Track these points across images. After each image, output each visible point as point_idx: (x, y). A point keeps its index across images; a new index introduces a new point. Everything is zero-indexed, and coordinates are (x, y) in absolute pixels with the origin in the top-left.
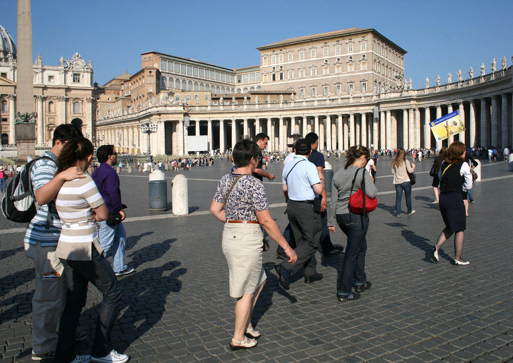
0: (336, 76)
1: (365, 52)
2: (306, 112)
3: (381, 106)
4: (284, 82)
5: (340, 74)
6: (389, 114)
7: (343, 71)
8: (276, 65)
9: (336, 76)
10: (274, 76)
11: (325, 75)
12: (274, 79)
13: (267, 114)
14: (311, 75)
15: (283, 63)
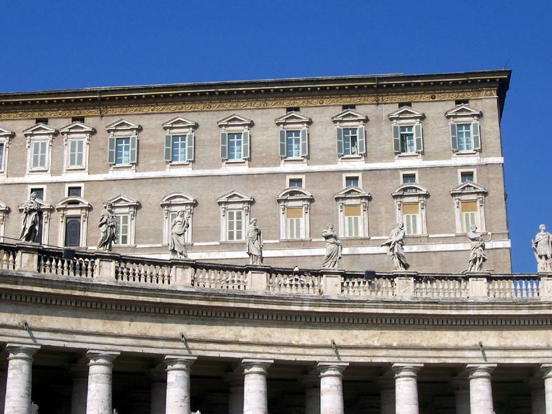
1: (473, 160)
2: (491, 338)
5: (365, 241)
7: (373, 228)
8: (47, 177)
11: (291, 243)
13: (247, 333)
14: (224, 237)
15: (84, 176)
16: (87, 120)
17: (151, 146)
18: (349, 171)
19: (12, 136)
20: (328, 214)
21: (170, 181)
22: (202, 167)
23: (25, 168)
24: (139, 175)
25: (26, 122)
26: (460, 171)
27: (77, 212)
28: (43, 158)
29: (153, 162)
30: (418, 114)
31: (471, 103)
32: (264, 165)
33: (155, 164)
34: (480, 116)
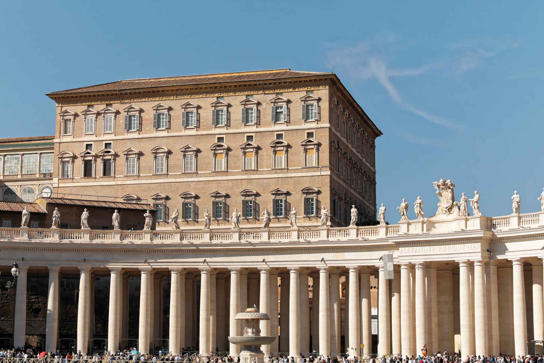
0: (245, 177)
3: (403, 251)
4: (113, 183)
6: (419, 273)
8: (93, 138)
9: (245, 177)
10: (88, 166)
12: (87, 173)
15: (112, 137)
16: (114, 105)
17: (147, 119)
18: (248, 133)
19: (76, 115)
20: (236, 157)
21: (157, 139)
22: (173, 132)
23: (83, 133)
24: (140, 136)
25: (82, 107)
26: (306, 131)
27: (110, 157)
28: (91, 127)
29: (148, 128)
30: (285, 99)
31: (315, 92)
32: (204, 130)
33: (149, 130)
34: (319, 100)
